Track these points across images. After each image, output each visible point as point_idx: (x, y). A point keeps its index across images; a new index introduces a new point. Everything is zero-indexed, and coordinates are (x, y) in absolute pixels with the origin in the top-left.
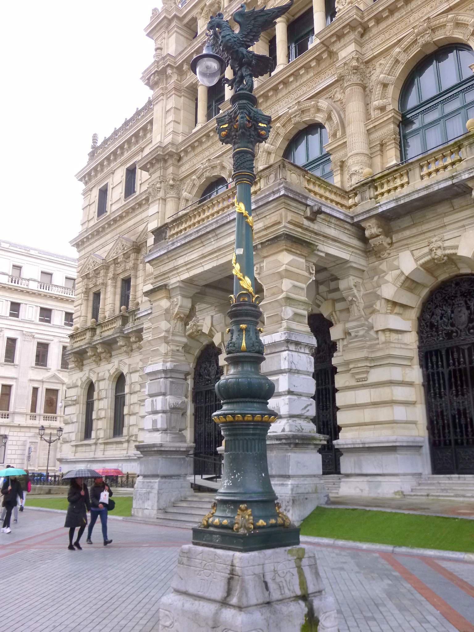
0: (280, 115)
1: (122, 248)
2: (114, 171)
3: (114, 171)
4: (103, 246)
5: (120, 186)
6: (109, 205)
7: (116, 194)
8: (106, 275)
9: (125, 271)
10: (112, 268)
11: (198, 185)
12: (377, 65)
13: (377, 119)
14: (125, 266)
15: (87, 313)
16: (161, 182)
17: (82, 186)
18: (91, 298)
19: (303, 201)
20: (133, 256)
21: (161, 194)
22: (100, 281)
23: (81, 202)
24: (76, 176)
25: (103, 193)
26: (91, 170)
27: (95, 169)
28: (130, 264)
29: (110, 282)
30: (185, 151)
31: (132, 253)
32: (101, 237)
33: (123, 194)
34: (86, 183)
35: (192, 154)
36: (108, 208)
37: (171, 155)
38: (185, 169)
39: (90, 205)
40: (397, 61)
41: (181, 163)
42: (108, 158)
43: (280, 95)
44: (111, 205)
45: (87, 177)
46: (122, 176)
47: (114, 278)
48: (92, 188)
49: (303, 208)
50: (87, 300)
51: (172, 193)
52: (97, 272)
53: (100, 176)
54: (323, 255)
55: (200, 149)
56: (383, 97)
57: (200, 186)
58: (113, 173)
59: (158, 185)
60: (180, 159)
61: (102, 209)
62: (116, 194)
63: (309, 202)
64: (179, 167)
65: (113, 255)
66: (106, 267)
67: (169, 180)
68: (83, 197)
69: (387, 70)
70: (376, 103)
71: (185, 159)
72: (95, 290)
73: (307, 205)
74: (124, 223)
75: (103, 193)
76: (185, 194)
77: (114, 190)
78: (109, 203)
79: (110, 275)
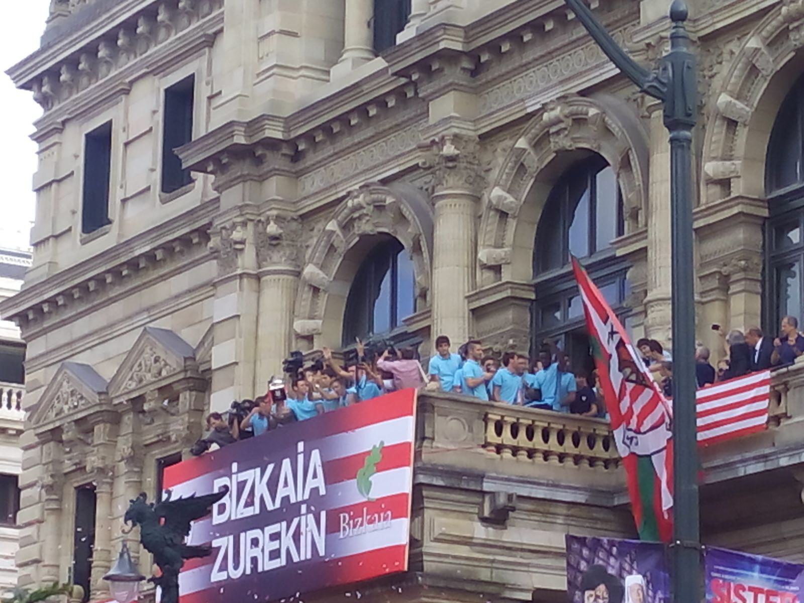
0: (529, 110)
1: (154, 371)
2: (132, 83)
3: (132, 83)
4: (103, 335)
5: (146, 142)
6: (118, 202)
7: (137, 166)
8: (112, 444)
9: (164, 440)
10: (128, 419)
11: (342, 248)
12: (726, 56)
13: (711, 210)
14: (167, 424)
15: (58, 555)
16: (244, 224)
17: (28, 109)
18: (70, 504)
19: (473, 487)
20: (186, 399)
21: (247, 261)
22: (93, 461)
23: (27, 160)
24: (9, 72)
25: (99, 145)
26: (61, 62)
27: (72, 62)
28: (178, 427)
29: (123, 467)
30: (309, 136)
31: (185, 389)
32: (94, 309)
33: (157, 175)
34: (44, 101)
35: (329, 150)
36: (114, 209)
37: (272, 144)
38: (315, 186)
39: (59, 181)
40: (753, 71)
41: (301, 166)
42: (110, 38)
43: (530, 55)
44: (124, 201)
45: (46, 78)
46: (154, 112)
47: (135, 459)
48: (64, 123)
49: (478, 499)
50: (59, 511)
51: (279, 261)
52: (85, 426)
53: (89, 90)
54: (528, 597)
55: (346, 141)
56: (727, 157)
57: (350, 254)
58: (127, 92)
59: (237, 235)
60: (297, 156)
61: (95, 215)
62: (137, 166)
63: (487, 486)
64: (298, 174)
65: (128, 388)
66: (114, 417)
67: (268, 221)
68: (35, 146)
69: (735, 84)
70: (710, 168)
71: (311, 159)
72: (80, 480)
73: (483, 493)
74: (163, 278)
75: (99, 145)
76: (310, 270)
77: (131, 148)
78: (116, 194)
79: (124, 446)
